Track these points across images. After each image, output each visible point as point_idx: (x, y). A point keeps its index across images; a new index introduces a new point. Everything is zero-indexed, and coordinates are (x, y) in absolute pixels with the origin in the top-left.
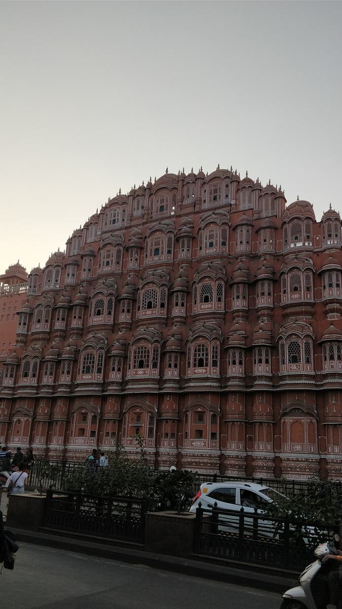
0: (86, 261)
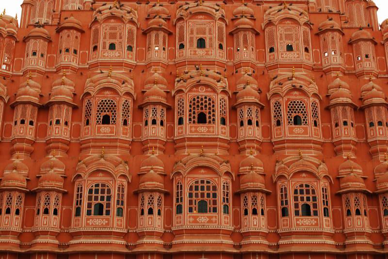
0: (68, 36)
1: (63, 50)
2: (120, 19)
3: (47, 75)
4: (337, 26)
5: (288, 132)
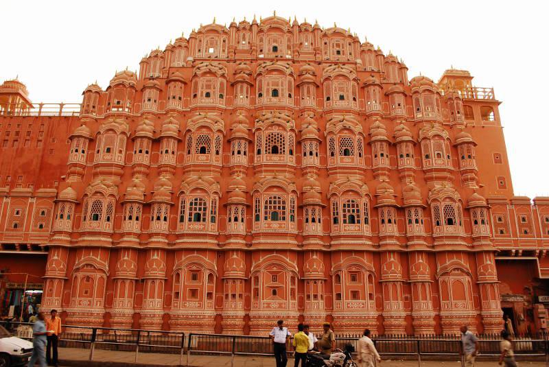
1: (171, 98)
2: (214, 74)
3: (158, 116)
4: (377, 82)
5: (339, 160)
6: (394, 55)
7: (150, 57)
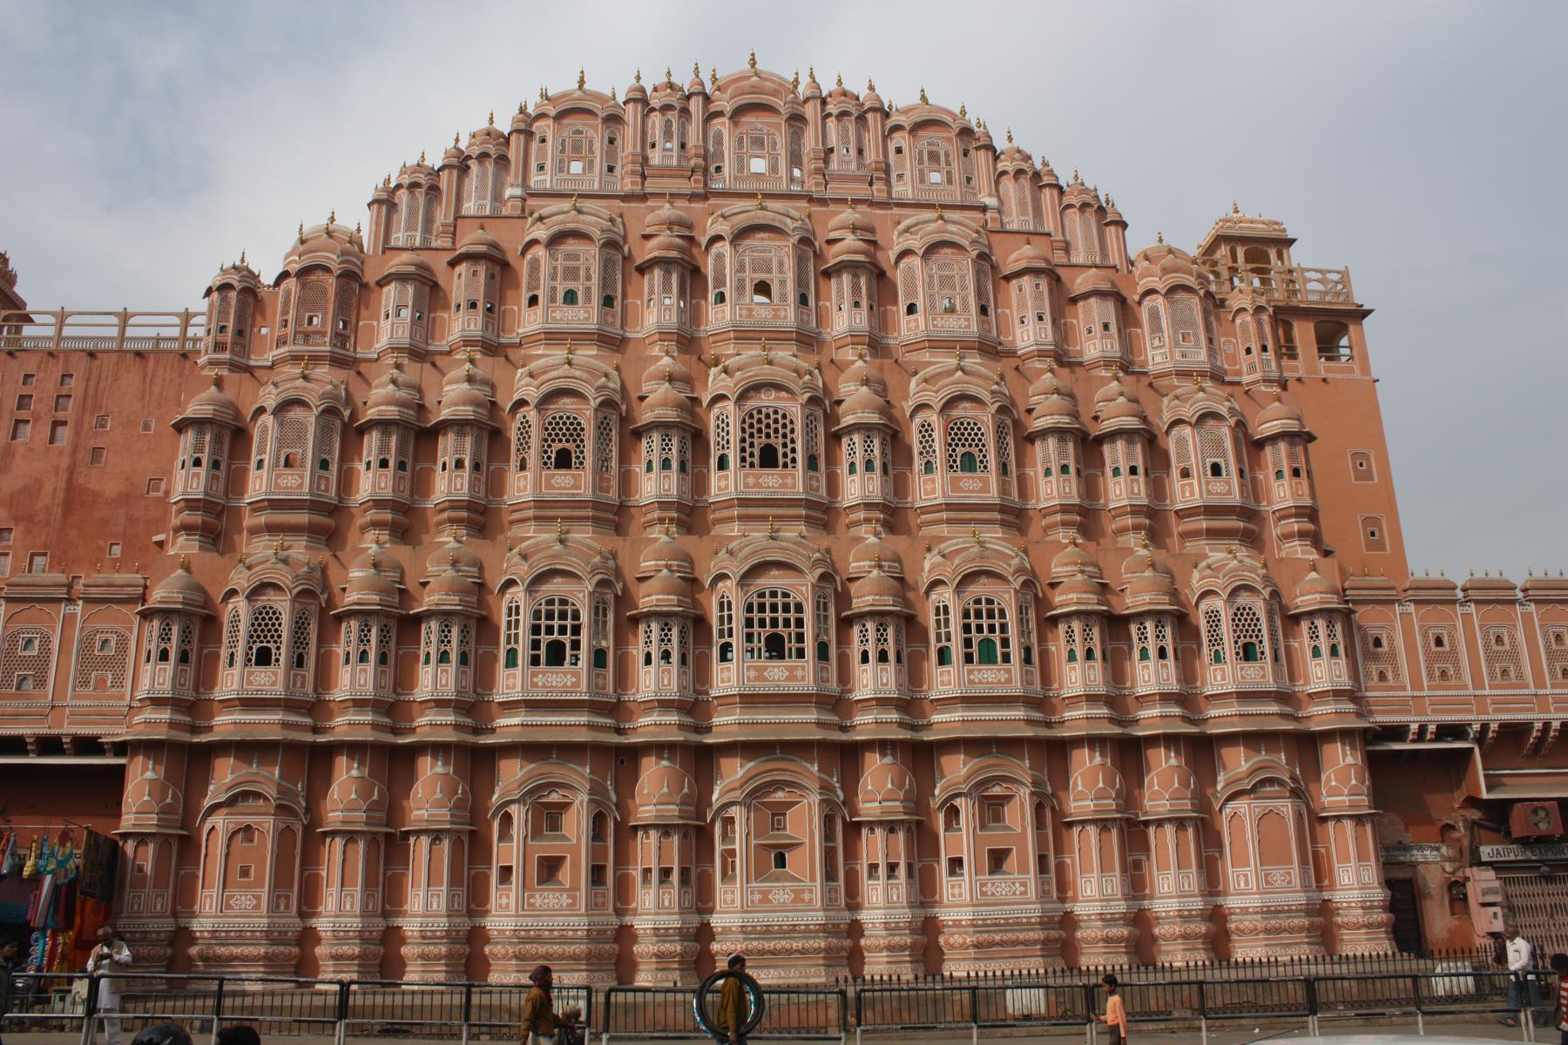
6: (1089, 185)
7: (399, 186)
